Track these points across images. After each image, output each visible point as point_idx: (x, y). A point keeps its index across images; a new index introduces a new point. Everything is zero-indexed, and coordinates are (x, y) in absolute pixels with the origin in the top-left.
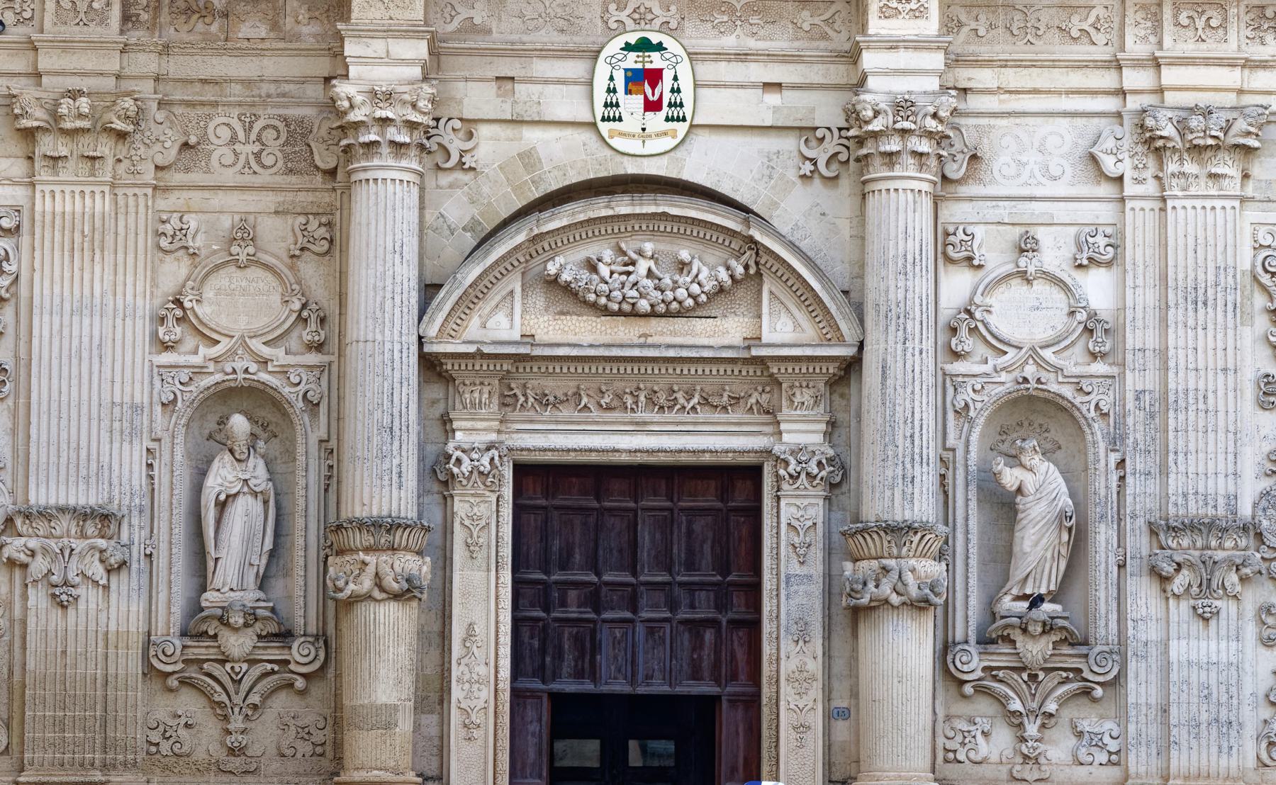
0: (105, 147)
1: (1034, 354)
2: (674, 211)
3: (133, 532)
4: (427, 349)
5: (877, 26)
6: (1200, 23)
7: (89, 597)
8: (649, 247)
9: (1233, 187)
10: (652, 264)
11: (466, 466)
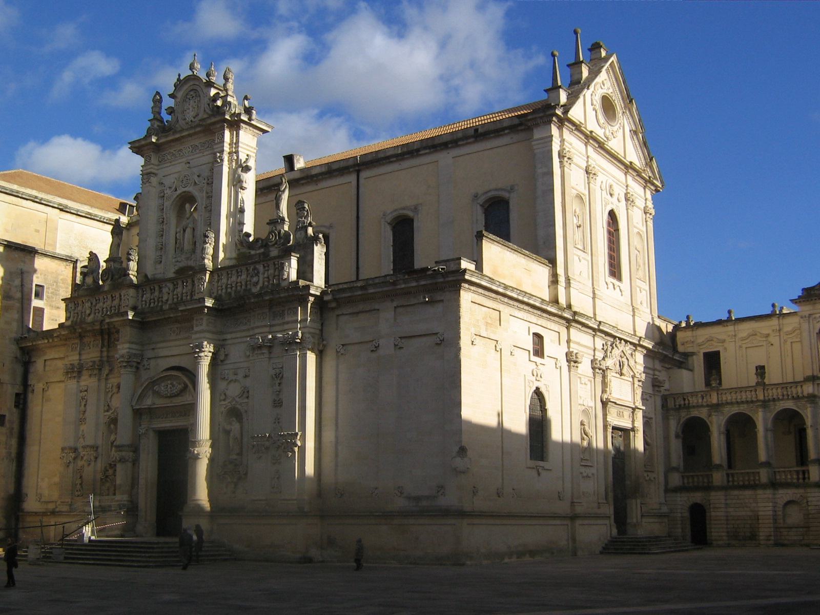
0: (96, 372)
1: (234, 399)
2: (173, 374)
3: (100, 450)
4: (134, 408)
5: (196, 329)
6: (262, 318)
7: (93, 463)
8: (169, 382)
9: (267, 355)
10: (171, 386)
11: (141, 433)
